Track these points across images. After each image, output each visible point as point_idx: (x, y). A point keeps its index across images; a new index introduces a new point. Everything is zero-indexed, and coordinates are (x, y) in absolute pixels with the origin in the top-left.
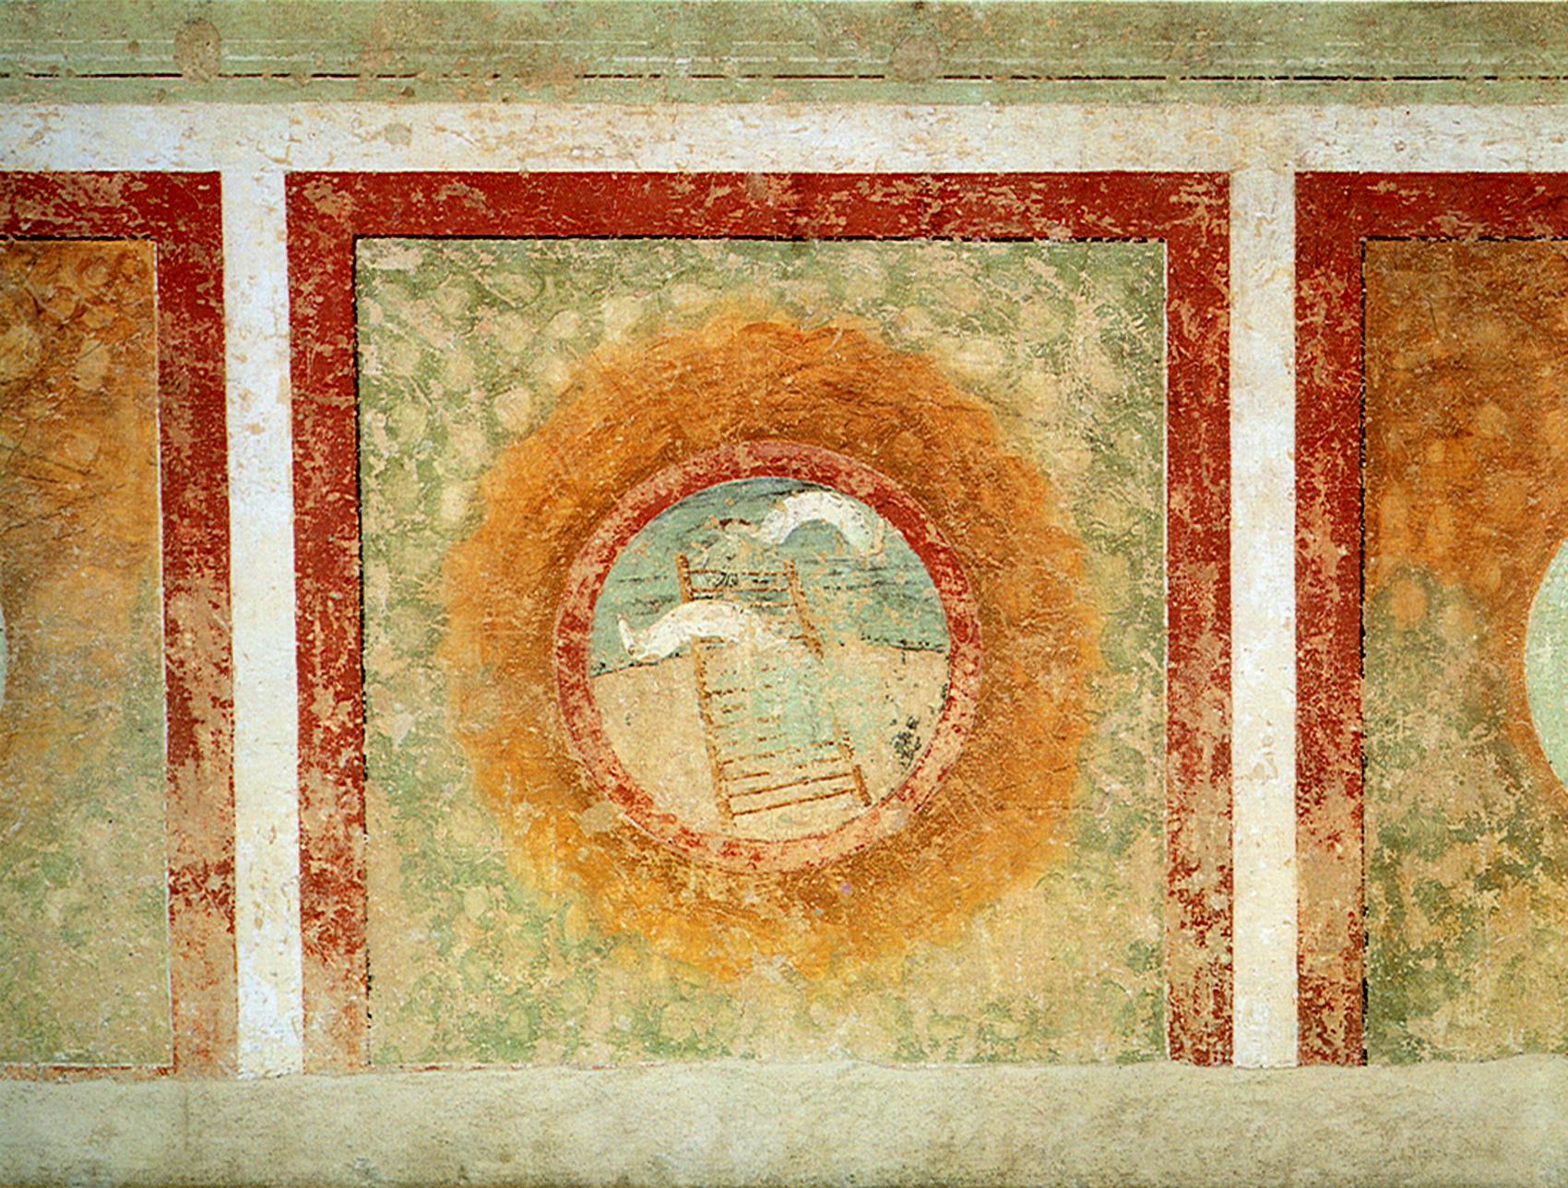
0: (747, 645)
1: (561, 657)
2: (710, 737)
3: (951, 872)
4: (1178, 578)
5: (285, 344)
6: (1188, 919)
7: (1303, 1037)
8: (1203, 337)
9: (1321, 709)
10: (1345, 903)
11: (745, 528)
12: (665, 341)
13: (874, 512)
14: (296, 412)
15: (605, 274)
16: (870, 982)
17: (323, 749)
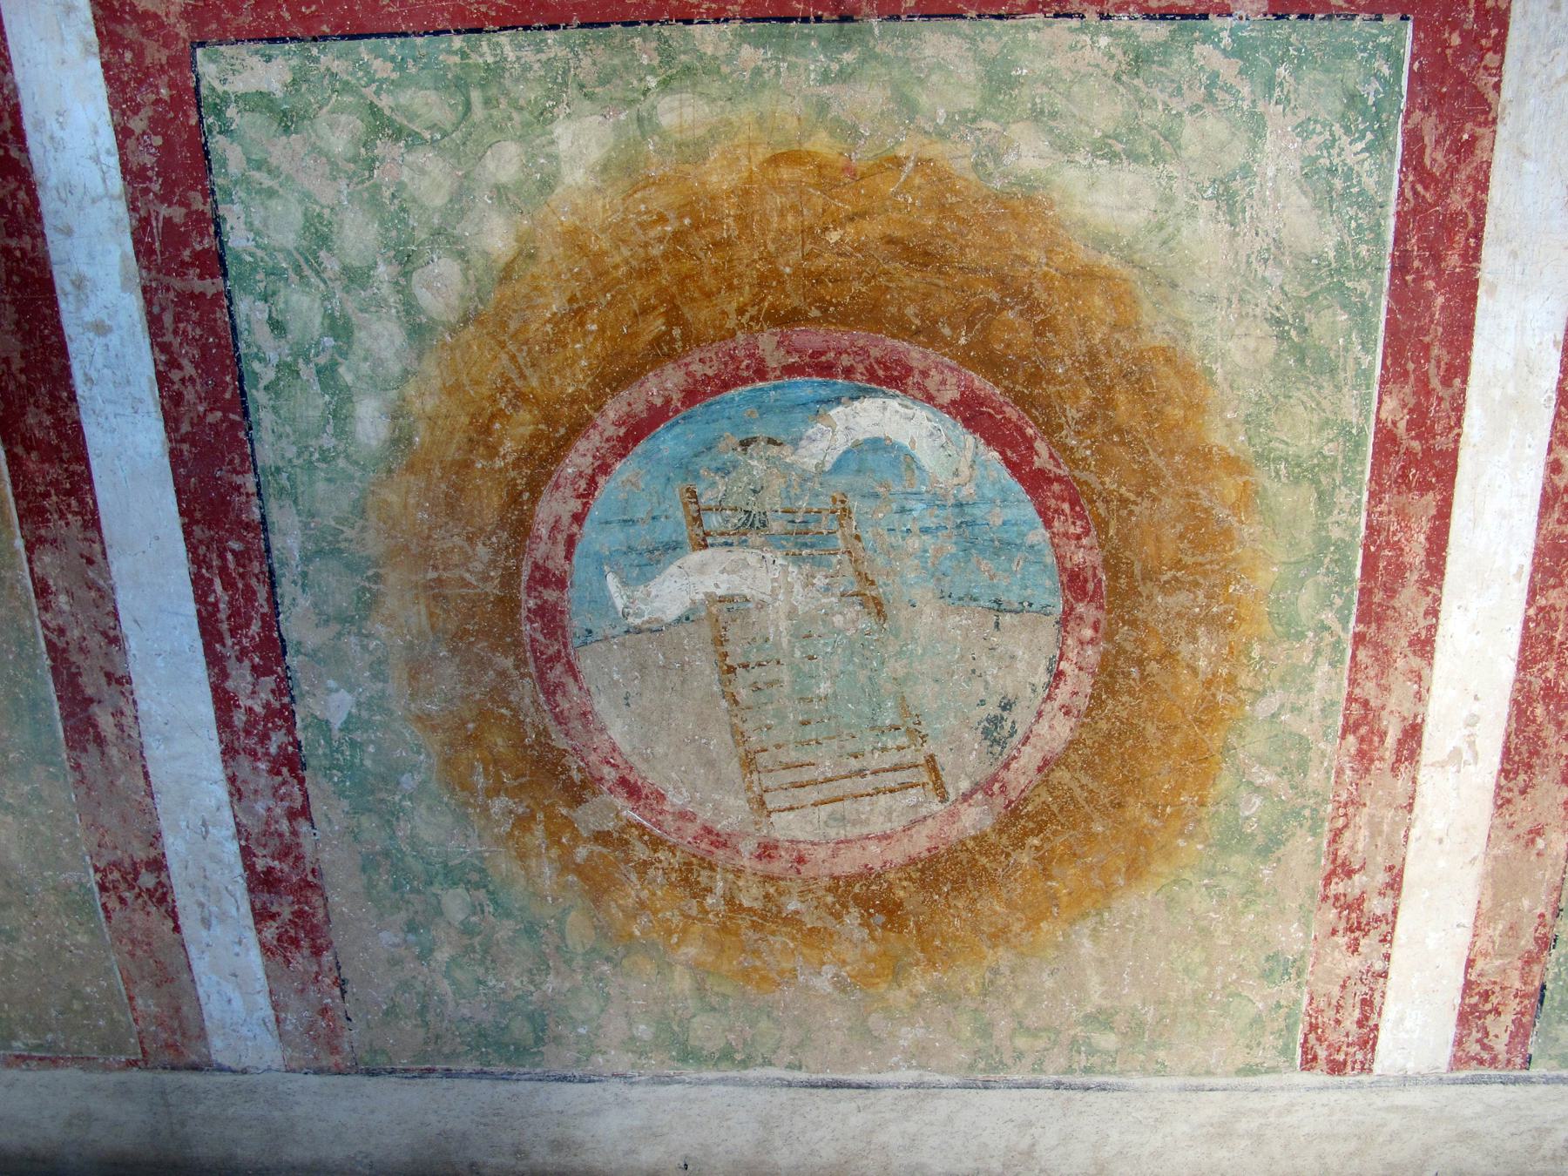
0: (782, 604)
1: (532, 622)
2: (735, 720)
3: (1049, 877)
4: (1381, 514)
5: (121, 209)
6: (1342, 926)
7: (1459, 1042)
8: (1452, 169)
9: (1547, 680)
10: (1533, 904)
11: (774, 450)
12: (649, 182)
13: (960, 425)
14: (149, 302)
15: (559, 81)
16: (942, 994)
17: (248, 733)
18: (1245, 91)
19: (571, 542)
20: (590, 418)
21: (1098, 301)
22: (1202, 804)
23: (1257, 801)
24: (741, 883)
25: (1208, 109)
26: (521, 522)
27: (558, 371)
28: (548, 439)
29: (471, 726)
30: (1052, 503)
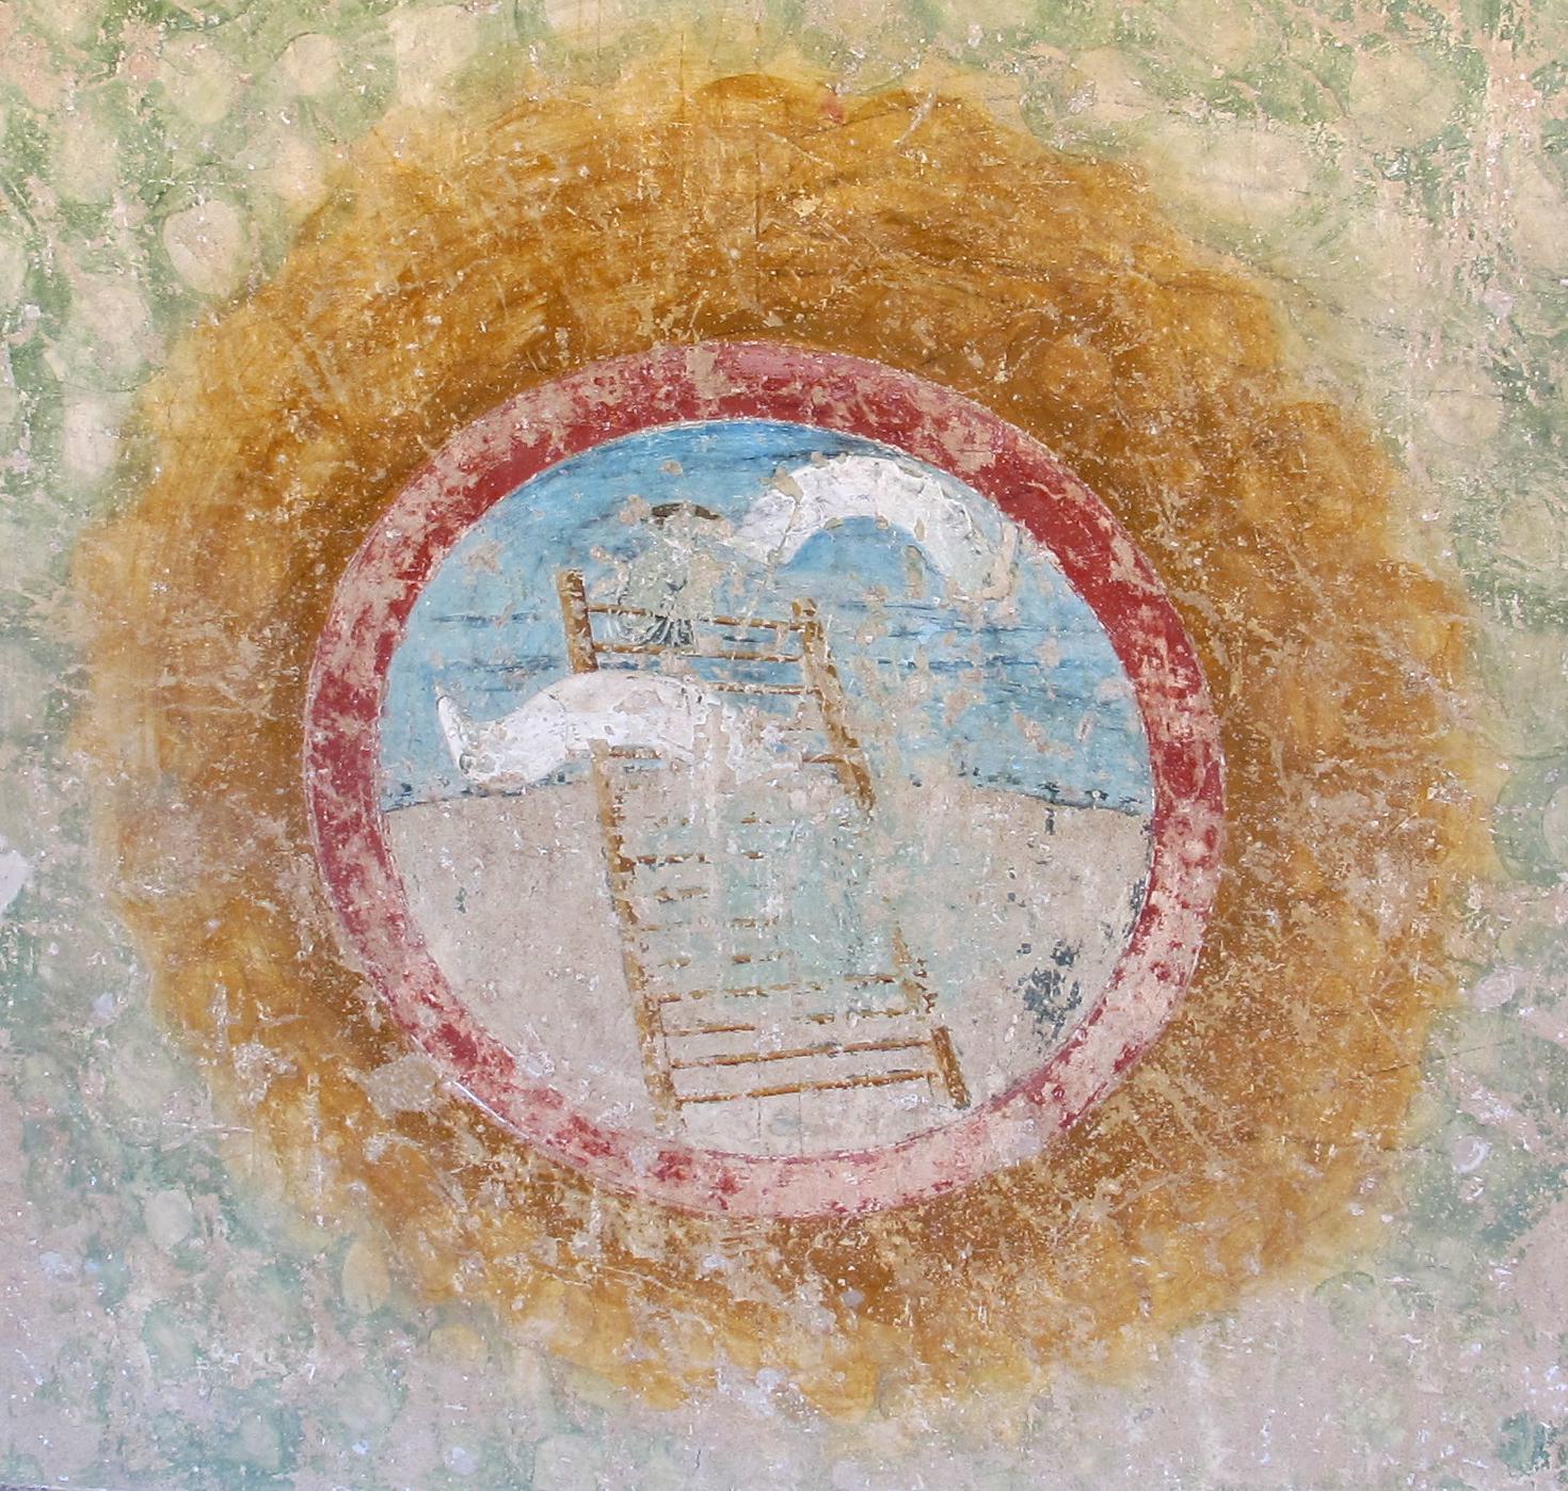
0: (709, 766)
1: (319, 766)
2: (630, 947)
3: (1136, 1250)
11: (706, 526)
12: (527, 109)
13: (994, 506)
16: (957, 1437)
18: (1453, 16)
19: (386, 645)
20: (423, 457)
21: (1215, 328)
22: (1388, 1147)
23: (1481, 1148)
24: (630, 1217)
25: (1392, 42)
26: (311, 609)
27: (380, 381)
28: (359, 485)
29: (212, 924)
30: (1139, 636)
